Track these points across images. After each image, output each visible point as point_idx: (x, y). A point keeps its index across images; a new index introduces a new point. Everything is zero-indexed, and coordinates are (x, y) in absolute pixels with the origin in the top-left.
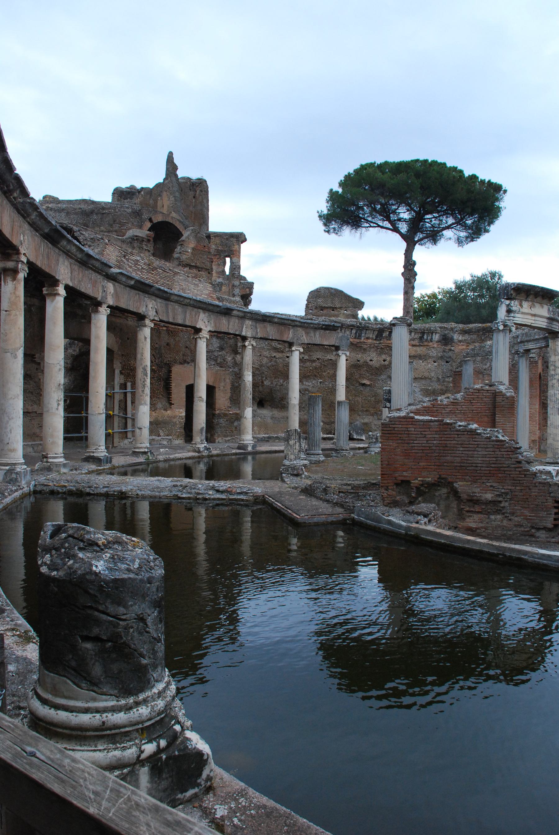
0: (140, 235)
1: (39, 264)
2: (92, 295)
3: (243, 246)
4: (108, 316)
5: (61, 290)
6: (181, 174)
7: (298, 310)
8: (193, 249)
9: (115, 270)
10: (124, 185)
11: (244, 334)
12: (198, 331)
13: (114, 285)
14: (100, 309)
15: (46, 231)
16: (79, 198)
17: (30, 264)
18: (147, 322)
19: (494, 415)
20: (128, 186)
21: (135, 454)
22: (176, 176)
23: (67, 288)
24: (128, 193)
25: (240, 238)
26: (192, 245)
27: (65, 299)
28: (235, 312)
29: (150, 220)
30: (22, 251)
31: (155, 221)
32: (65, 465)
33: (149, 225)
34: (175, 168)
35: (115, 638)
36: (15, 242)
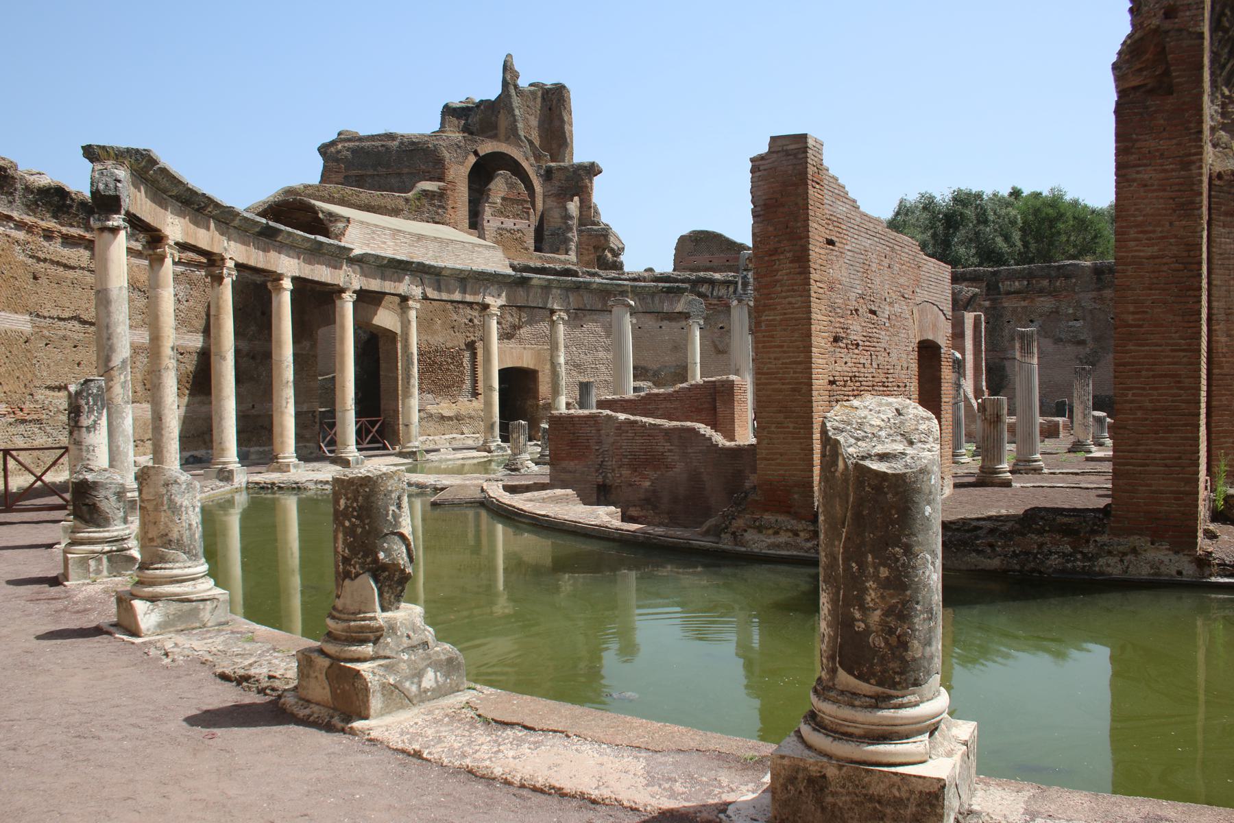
0: (430, 188)
1: (252, 263)
2: (329, 281)
3: (597, 180)
4: (354, 303)
5: (287, 284)
6: (523, 83)
7: (664, 264)
8: (504, 199)
9: (357, 251)
10: (456, 100)
11: (549, 306)
12: (485, 307)
13: (361, 268)
14: (344, 295)
15: (258, 230)
16: (382, 131)
17: (239, 266)
18: (410, 303)
19: (715, 400)
20: (463, 99)
21: (401, 455)
22: (516, 86)
23: (296, 280)
24: (462, 109)
25: (592, 170)
26: (503, 194)
27: (292, 292)
28: (534, 282)
29: (476, 153)
30: (227, 256)
31: (481, 153)
32: (296, 466)
33: (472, 159)
34: (516, 75)
35: (94, 504)
36: (215, 251)
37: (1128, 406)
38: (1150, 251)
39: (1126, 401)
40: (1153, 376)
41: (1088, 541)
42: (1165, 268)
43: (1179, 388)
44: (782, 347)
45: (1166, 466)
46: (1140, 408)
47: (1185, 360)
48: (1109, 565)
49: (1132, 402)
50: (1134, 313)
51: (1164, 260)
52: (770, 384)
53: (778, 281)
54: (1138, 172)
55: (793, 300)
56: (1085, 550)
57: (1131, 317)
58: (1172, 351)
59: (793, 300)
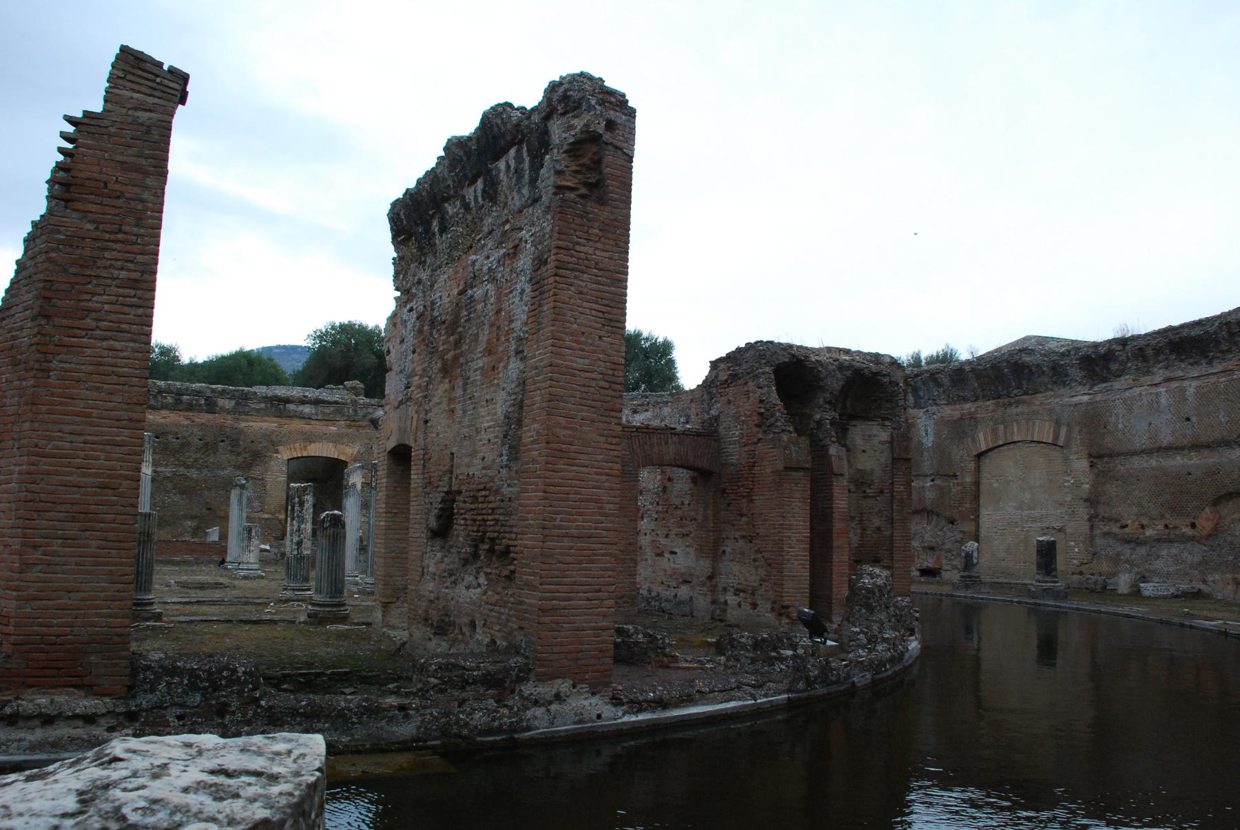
37: (555, 532)
38: (581, 363)
39: (554, 527)
40: (581, 501)
41: (513, 692)
42: (593, 383)
43: (600, 514)
44: (89, 415)
45: (588, 599)
46: (567, 535)
47: (607, 484)
48: (535, 718)
49: (560, 528)
50: (565, 428)
51: (593, 375)
52: (57, 473)
53: (90, 310)
54: (576, 278)
55: (117, 345)
56: (510, 703)
57: (563, 432)
58: (597, 474)
59: (117, 345)
